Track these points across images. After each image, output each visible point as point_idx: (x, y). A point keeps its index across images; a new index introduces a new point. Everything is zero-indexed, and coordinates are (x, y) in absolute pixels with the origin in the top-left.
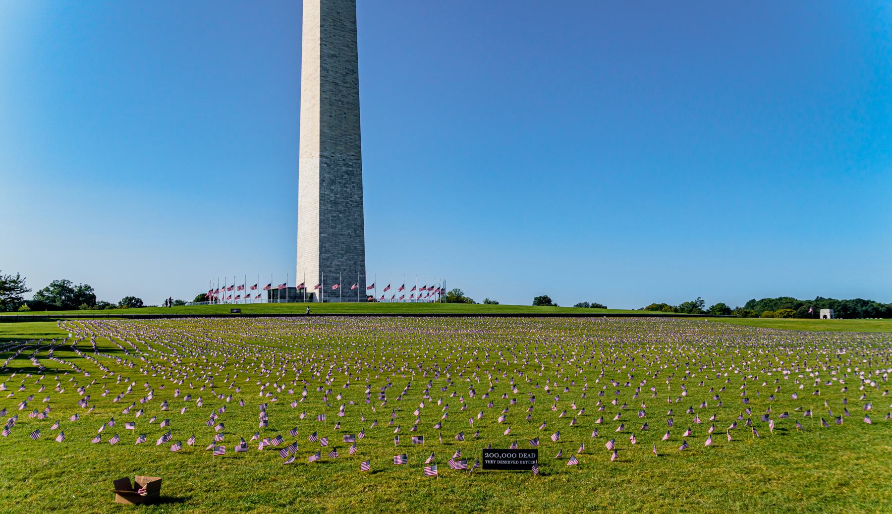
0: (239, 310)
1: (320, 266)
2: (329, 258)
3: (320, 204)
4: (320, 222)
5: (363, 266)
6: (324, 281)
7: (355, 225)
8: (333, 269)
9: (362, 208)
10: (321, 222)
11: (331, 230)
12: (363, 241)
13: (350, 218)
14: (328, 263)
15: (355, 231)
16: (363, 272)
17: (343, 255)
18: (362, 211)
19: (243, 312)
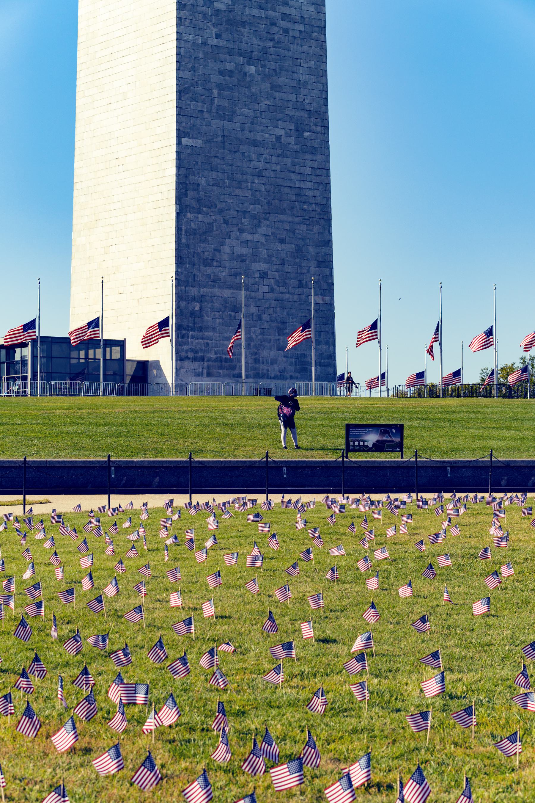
0: (392, 435)
1: (180, 259)
2: (209, 230)
3: (180, 21)
4: (180, 93)
5: (326, 263)
6: (188, 322)
7: (300, 107)
8: (223, 273)
9: (322, 44)
10: (183, 91)
11: (217, 123)
12: (326, 170)
13: (283, 80)
14: (207, 249)
15: (299, 131)
16: (326, 287)
17: (257, 221)
18: (322, 57)
19: (425, 445)
